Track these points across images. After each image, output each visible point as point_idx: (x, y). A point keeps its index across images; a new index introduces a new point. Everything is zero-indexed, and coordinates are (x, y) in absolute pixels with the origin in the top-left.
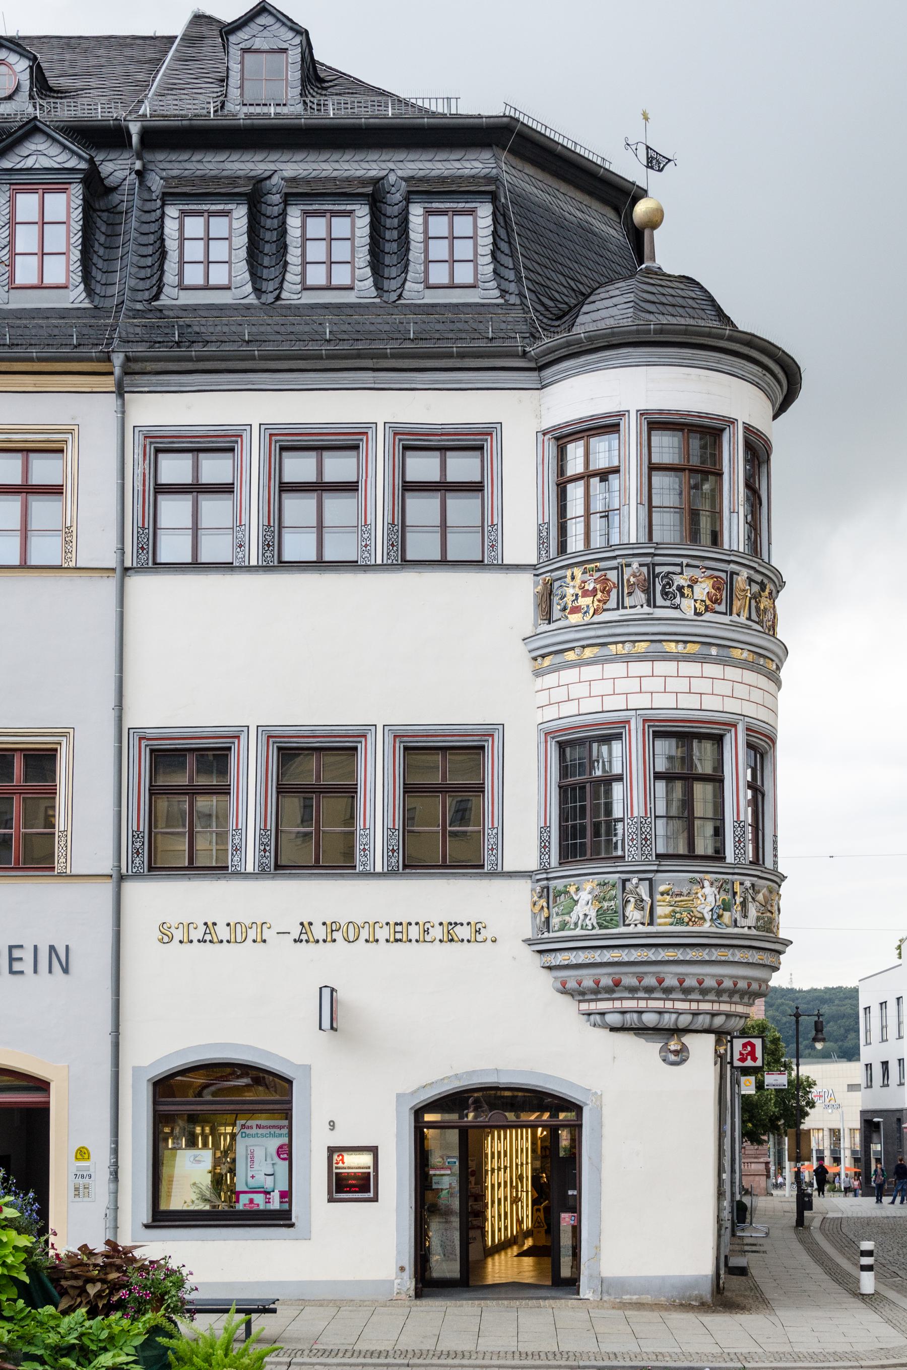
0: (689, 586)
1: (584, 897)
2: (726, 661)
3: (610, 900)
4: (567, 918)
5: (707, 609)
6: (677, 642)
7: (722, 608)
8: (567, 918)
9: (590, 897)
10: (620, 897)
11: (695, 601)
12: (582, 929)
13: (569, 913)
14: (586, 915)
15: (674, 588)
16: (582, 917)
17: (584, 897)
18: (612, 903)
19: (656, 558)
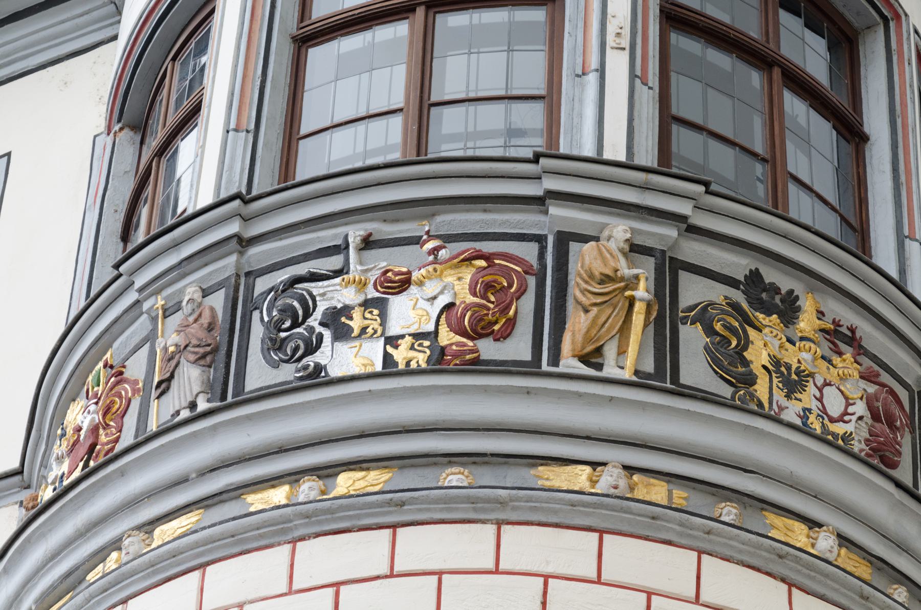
0: (367, 304)
2: (502, 503)
5: (440, 361)
6: (294, 477)
7: (518, 347)
11: (393, 341)
15: (314, 321)
19: (254, 251)
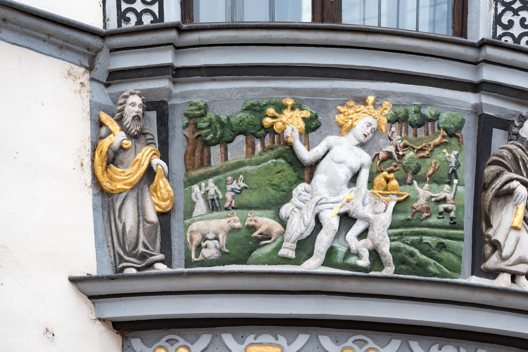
1: (342, 154)
3: (437, 180)
4: (265, 221)
8: (265, 221)
9: (366, 158)
10: (467, 174)
12: (325, 263)
13: (274, 206)
14: (347, 219)
16: (331, 221)
17: (342, 154)
18: (445, 191)
